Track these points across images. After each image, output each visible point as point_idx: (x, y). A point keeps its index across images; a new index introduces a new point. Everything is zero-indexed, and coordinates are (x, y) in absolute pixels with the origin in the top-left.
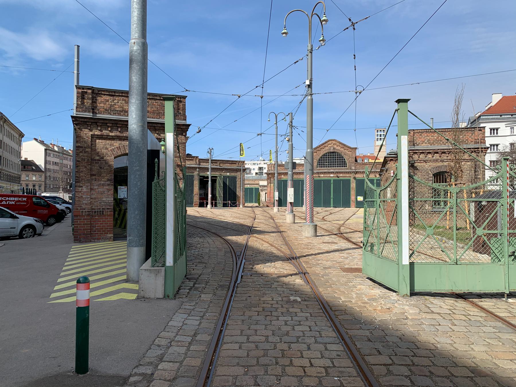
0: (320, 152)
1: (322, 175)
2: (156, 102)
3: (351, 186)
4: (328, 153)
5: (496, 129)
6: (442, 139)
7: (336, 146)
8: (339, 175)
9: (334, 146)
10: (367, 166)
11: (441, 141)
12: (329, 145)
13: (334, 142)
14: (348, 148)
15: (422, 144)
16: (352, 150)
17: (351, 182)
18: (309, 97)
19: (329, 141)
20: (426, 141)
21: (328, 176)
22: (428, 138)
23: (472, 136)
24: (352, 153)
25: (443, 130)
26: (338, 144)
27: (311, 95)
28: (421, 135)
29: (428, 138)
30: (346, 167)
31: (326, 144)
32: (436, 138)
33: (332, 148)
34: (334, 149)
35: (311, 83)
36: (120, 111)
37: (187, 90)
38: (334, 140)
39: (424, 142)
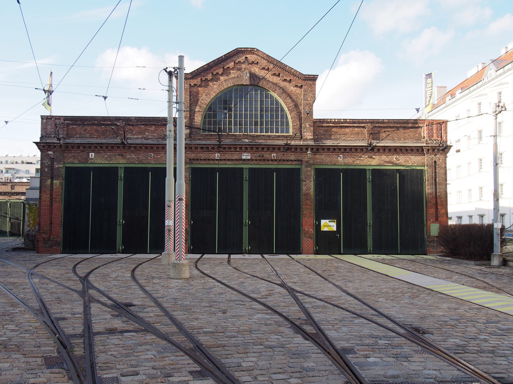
1: (217, 156)
3: (304, 188)
8: (267, 155)
10: (347, 130)
16: (304, 83)
17: (303, 177)
21: (236, 157)
24: (305, 91)
26: (264, 63)
30: (288, 131)
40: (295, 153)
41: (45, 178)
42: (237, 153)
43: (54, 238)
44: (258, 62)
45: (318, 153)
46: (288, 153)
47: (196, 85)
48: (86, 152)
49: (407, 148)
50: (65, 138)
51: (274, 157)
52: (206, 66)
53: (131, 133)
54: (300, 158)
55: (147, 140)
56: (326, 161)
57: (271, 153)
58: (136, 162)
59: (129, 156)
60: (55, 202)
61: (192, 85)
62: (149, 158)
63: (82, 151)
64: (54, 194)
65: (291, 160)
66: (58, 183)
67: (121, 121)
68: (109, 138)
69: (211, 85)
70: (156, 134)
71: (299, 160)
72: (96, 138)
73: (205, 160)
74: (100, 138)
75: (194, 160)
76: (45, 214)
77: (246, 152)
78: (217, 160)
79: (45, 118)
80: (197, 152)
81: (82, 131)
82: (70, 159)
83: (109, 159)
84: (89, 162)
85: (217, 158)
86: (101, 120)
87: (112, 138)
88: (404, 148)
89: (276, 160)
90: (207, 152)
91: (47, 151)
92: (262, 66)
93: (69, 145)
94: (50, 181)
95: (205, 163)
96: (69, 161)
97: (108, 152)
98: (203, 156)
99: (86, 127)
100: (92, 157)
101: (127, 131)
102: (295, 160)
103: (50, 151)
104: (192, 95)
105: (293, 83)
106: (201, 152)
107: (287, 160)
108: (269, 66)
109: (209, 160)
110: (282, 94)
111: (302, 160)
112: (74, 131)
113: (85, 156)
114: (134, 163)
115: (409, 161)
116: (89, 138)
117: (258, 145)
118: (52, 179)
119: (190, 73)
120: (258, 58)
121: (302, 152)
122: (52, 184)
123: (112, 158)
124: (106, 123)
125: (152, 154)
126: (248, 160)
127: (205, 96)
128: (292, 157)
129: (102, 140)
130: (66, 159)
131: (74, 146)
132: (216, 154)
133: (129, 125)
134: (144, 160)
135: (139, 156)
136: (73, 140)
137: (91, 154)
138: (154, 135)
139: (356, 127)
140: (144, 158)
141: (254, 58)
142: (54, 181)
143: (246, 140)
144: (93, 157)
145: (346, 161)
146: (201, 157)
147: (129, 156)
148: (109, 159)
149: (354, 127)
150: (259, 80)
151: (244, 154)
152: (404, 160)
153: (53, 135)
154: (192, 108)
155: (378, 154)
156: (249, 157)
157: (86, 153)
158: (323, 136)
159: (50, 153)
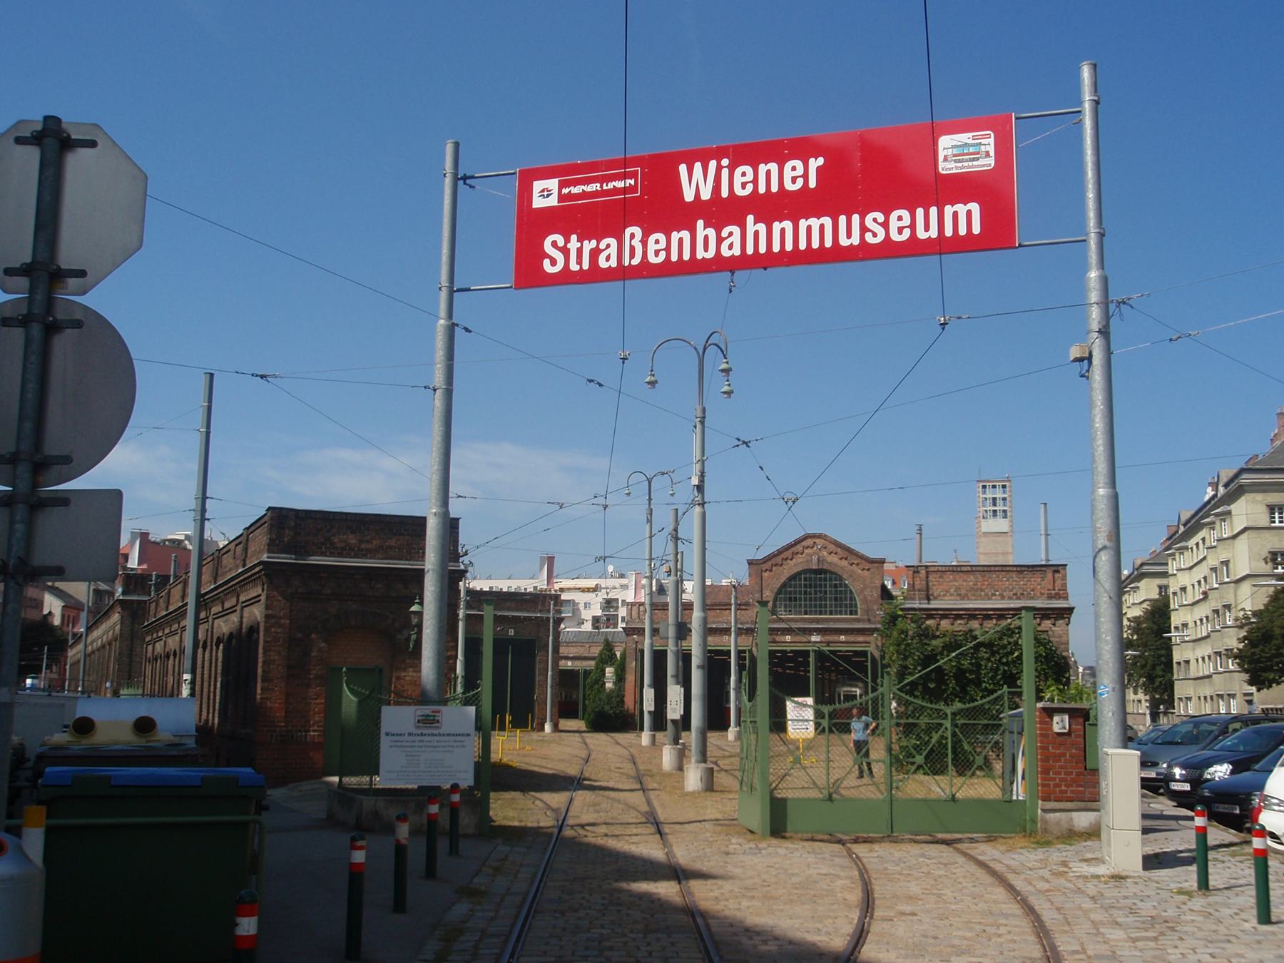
0: (781, 568)
1: (788, 638)
2: (405, 530)
4: (805, 571)
5: (1279, 509)
6: (984, 587)
7: (825, 554)
9: (821, 554)
11: (982, 590)
12: (806, 551)
13: (820, 542)
15: (945, 595)
18: (698, 509)
20: (952, 591)
21: (804, 640)
22: (957, 584)
23: (1043, 583)
25: (985, 569)
26: (832, 547)
27: (703, 504)
28: (941, 577)
29: (957, 584)
30: (856, 614)
31: (799, 548)
32: (971, 583)
33: (815, 558)
35: (702, 480)
36: (343, 549)
37: (460, 496)
38: (820, 536)
39: (947, 592)
105: (861, 566)
156: (818, 640)
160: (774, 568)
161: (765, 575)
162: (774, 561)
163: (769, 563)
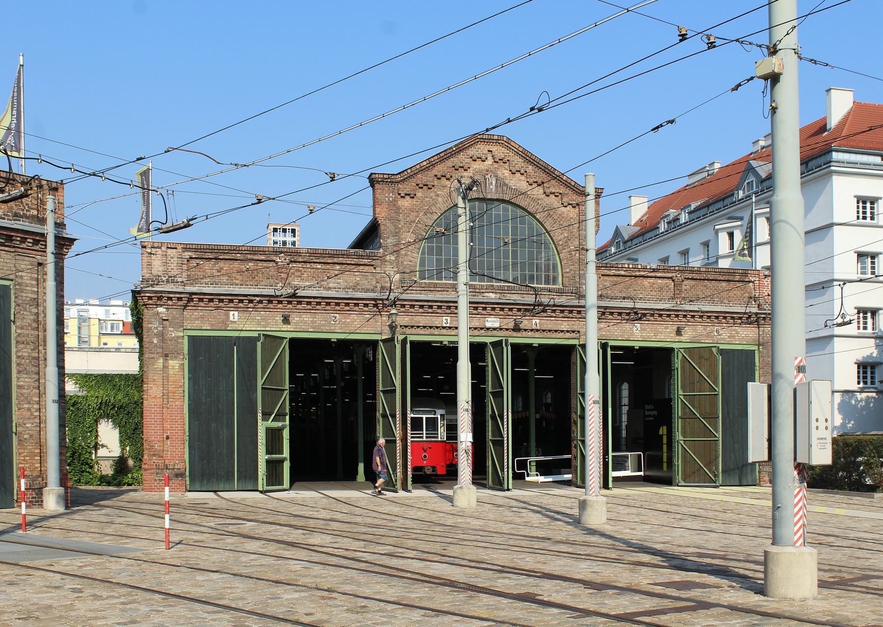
7: (507, 173)
9: (500, 174)
10: (646, 282)
12: (477, 166)
13: (499, 151)
14: (562, 190)
19: (476, 139)
26: (518, 162)
30: (555, 281)
34: (501, 184)
40: (569, 319)
41: (153, 355)
42: (478, 316)
43: (175, 465)
44: (508, 160)
45: (604, 321)
46: (558, 319)
47: (409, 195)
48: (224, 309)
49: (734, 315)
50: (187, 284)
51: (536, 325)
52: (425, 163)
53: (299, 277)
54: (576, 328)
55: (328, 291)
56: (616, 334)
57: (531, 318)
58: (310, 330)
59: (298, 319)
60: (172, 400)
61: (402, 195)
62: (332, 322)
63: (218, 308)
64: (171, 385)
65: (562, 331)
66: (178, 365)
67: (283, 255)
68: (263, 285)
69: (434, 197)
70: (342, 281)
71: (573, 332)
72: (241, 285)
73: (424, 327)
74: (247, 285)
75: (406, 327)
76: (157, 421)
77: (492, 315)
78: (444, 328)
79: (150, 246)
80: (413, 314)
81: (214, 271)
82: (196, 322)
83: (264, 323)
84: (228, 328)
85: (445, 325)
86: (248, 252)
87: (267, 286)
88: (730, 315)
89: (538, 330)
90: (430, 315)
91: (155, 306)
92: (515, 167)
93: (195, 296)
94: (162, 361)
95: (426, 333)
96: (194, 325)
97: (263, 310)
98: (423, 320)
99: (221, 264)
100: (234, 319)
101: (292, 274)
102: (568, 331)
103: (161, 306)
104: (401, 213)
105: (565, 200)
106: (419, 314)
107: (556, 331)
108: (526, 167)
109: (431, 327)
110: (547, 217)
111: (579, 332)
112: (200, 272)
113: (222, 317)
114: (307, 330)
115: (735, 336)
116: (228, 284)
117: (512, 304)
118: (166, 360)
119: (399, 173)
120: (508, 153)
121: (580, 318)
122: (165, 367)
123: (269, 321)
124: (256, 257)
125: (337, 315)
126: (495, 329)
127: (423, 215)
128: (565, 326)
129: (251, 288)
130: (189, 322)
131: (202, 297)
132: (444, 318)
133: (295, 262)
134: (324, 325)
135: (315, 319)
136: (200, 287)
137: (232, 313)
138: (339, 281)
139: (660, 278)
140: (324, 322)
141: (503, 153)
142: (170, 362)
143: (491, 294)
144: (236, 319)
145: (645, 334)
146: (419, 322)
147: (298, 319)
148: (264, 323)
149: (656, 277)
150: (511, 191)
151: (489, 319)
152: (729, 335)
153: (165, 277)
154: (403, 236)
155: (691, 324)
156: (497, 325)
157: (224, 312)
158: (609, 292)
159: (160, 310)
160: (419, 194)
161: (406, 203)
162: (421, 178)
163: (412, 183)
